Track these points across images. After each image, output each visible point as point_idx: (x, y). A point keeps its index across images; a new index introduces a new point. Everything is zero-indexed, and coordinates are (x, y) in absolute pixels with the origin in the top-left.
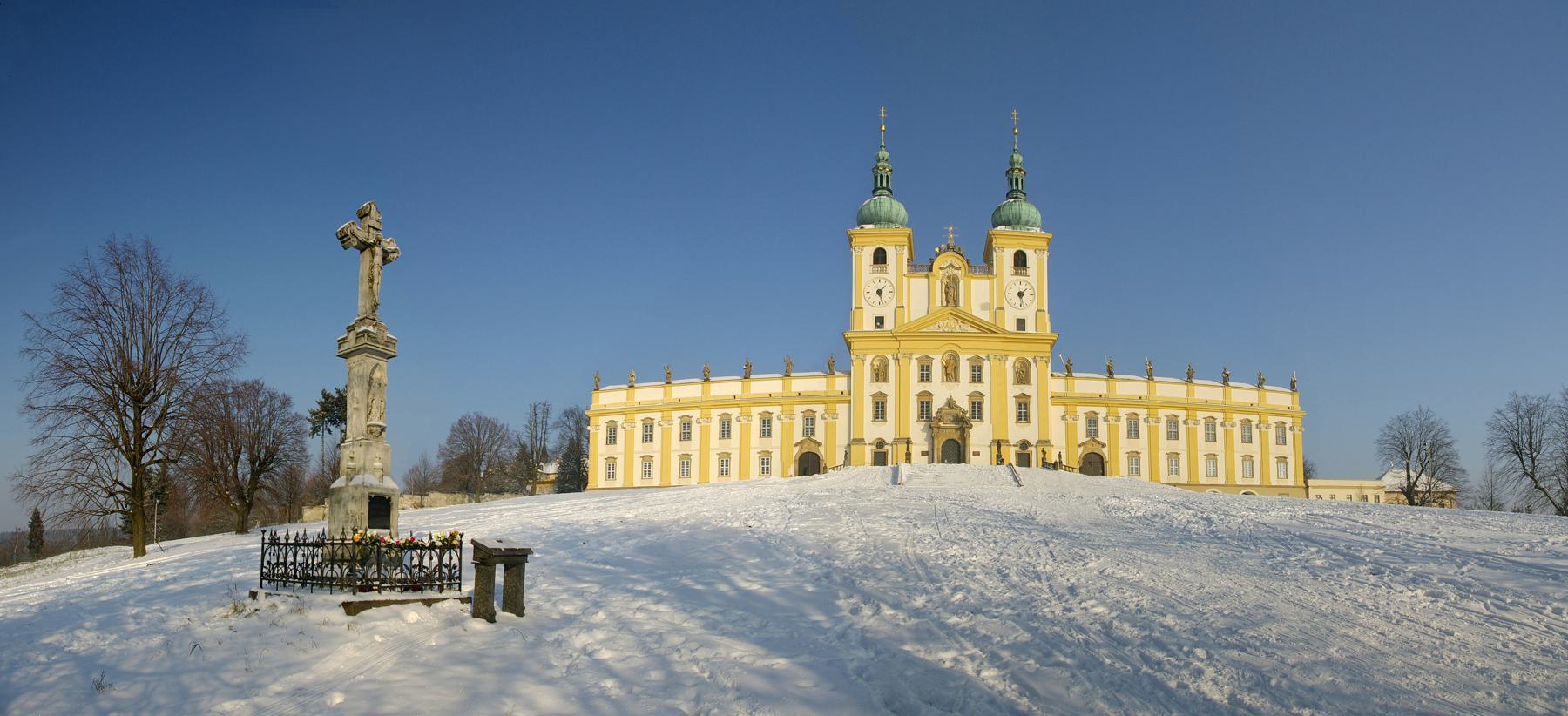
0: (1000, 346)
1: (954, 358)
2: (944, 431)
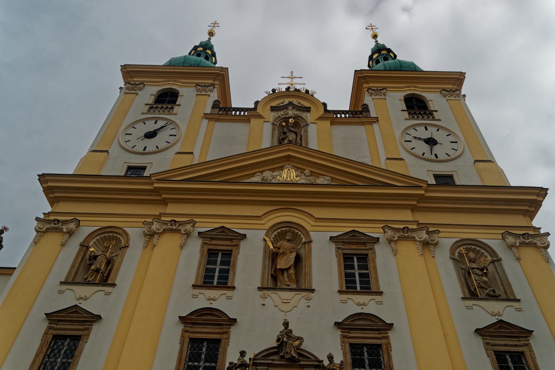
0: (407, 215)
1: (295, 238)
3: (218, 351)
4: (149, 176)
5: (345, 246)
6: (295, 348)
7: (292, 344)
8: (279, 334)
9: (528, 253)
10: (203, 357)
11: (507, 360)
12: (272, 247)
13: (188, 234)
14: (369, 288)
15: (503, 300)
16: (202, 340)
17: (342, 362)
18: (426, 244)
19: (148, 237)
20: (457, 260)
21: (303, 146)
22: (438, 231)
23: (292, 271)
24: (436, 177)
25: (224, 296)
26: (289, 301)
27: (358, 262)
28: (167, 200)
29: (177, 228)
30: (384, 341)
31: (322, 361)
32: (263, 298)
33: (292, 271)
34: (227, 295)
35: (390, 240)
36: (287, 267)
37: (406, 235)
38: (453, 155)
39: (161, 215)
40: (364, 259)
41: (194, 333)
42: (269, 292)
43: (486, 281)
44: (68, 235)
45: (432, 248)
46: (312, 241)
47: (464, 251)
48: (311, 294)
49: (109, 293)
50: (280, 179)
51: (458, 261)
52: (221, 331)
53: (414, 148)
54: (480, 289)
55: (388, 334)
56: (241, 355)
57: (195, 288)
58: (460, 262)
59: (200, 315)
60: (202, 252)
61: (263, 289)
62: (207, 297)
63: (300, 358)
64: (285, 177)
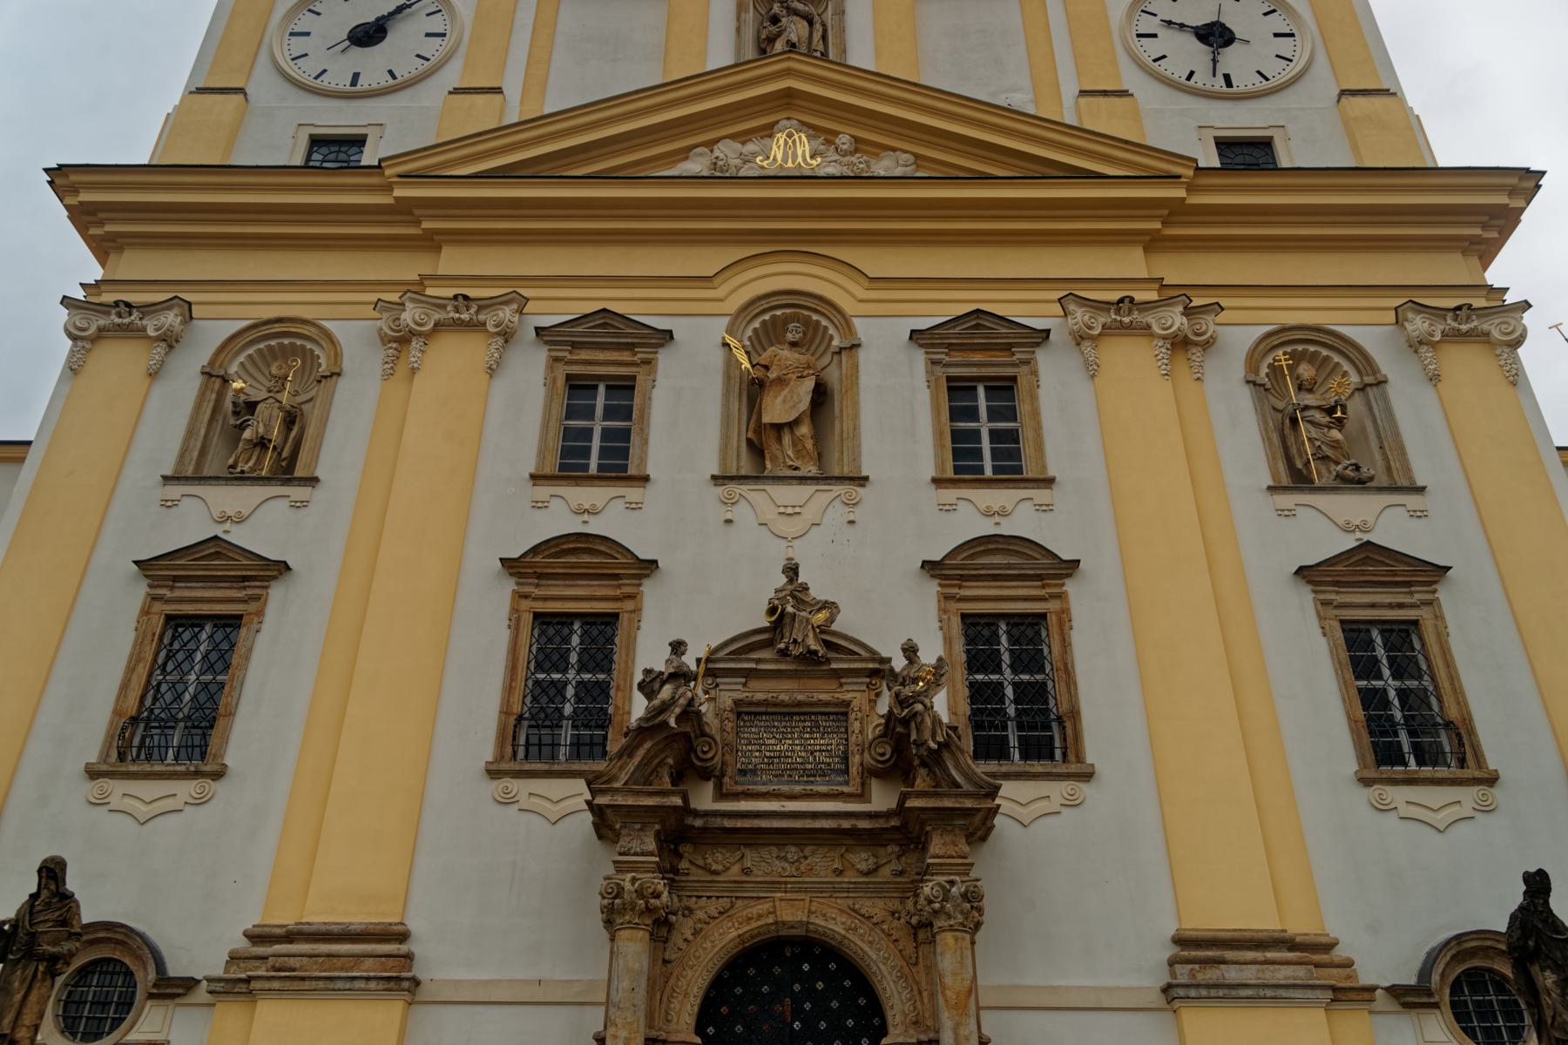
0: (1131, 263)
1: (811, 337)
2: (728, 864)
3: (613, 643)
4: (376, 164)
5: (954, 357)
6: (818, 630)
7: (808, 620)
8: (772, 595)
9: (1462, 363)
10: (573, 658)
11: (1372, 641)
12: (746, 364)
13: (507, 335)
14: (1019, 470)
15: (1381, 490)
16: (569, 618)
17: (940, 659)
18: (1180, 343)
19: (394, 345)
20: (1263, 385)
21: (831, 58)
22: (1216, 306)
23: (804, 430)
24: (1223, 145)
25: (620, 504)
26: (797, 510)
27: (988, 400)
28: (436, 237)
29: (475, 318)
30: (1052, 606)
31: (889, 660)
32: (726, 504)
33: (804, 430)
34: (627, 500)
35: (1080, 336)
36: (791, 419)
37: (1126, 320)
38: (1278, 77)
39: (426, 282)
40: (1004, 389)
41: (545, 599)
42: (744, 489)
43: (1337, 441)
44: (164, 345)
45: (1196, 354)
46: (859, 345)
47: (1285, 360)
48: (858, 489)
49: (303, 504)
50: (765, 164)
51: (1266, 390)
52: (618, 592)
53: (1164, 57)
54: (1319, 462)
55: (1064, 588)
56: (672, 651)
57: (538, 482)
58: (1272, 391)
59: (556, 553)
60: (550, 383)
61: (726, 482)
62: (574, 505)
63: (831, 655)
64: (779, 157)
